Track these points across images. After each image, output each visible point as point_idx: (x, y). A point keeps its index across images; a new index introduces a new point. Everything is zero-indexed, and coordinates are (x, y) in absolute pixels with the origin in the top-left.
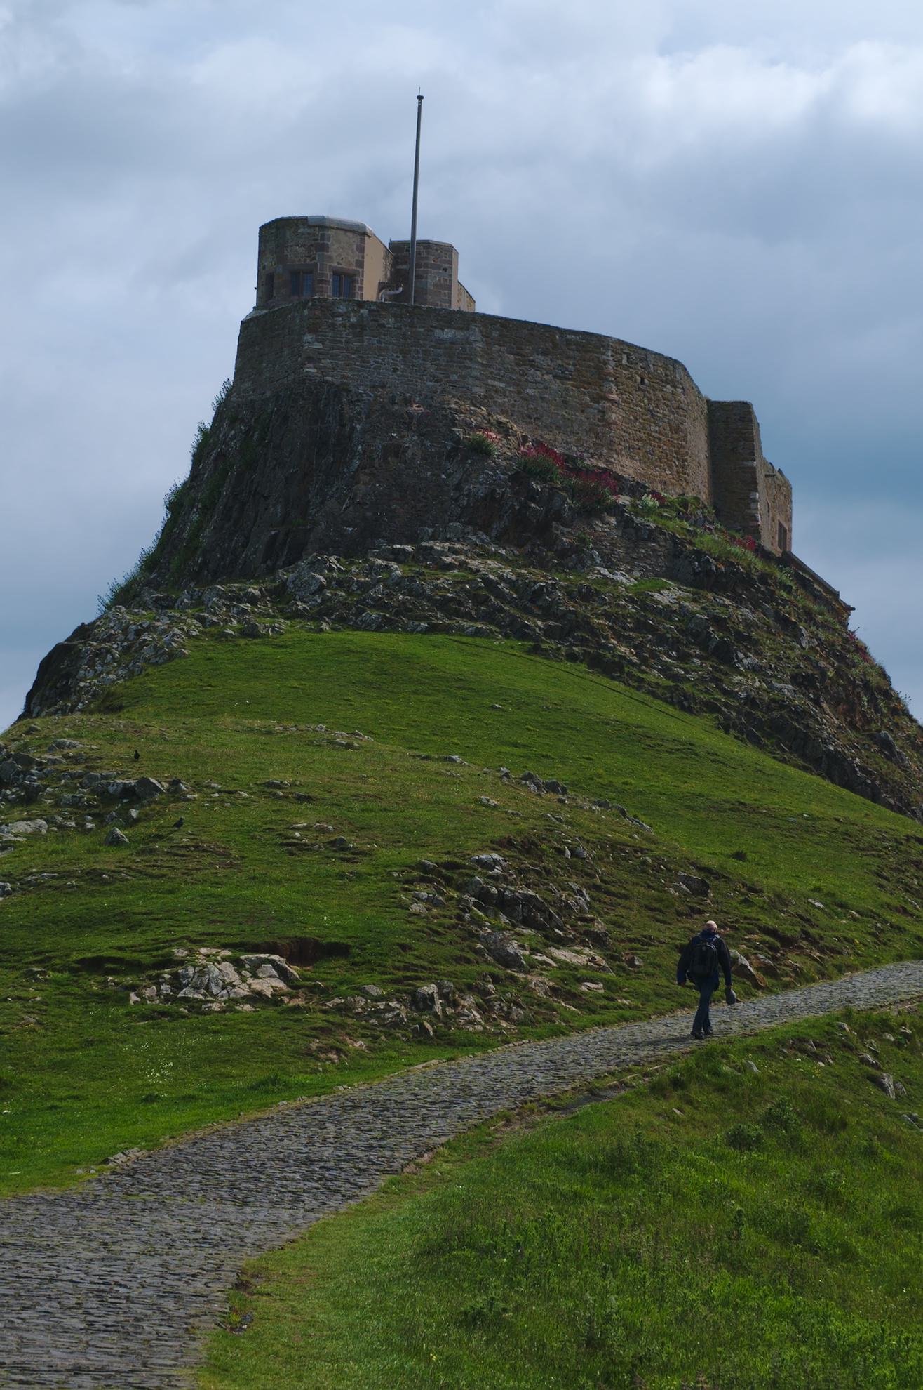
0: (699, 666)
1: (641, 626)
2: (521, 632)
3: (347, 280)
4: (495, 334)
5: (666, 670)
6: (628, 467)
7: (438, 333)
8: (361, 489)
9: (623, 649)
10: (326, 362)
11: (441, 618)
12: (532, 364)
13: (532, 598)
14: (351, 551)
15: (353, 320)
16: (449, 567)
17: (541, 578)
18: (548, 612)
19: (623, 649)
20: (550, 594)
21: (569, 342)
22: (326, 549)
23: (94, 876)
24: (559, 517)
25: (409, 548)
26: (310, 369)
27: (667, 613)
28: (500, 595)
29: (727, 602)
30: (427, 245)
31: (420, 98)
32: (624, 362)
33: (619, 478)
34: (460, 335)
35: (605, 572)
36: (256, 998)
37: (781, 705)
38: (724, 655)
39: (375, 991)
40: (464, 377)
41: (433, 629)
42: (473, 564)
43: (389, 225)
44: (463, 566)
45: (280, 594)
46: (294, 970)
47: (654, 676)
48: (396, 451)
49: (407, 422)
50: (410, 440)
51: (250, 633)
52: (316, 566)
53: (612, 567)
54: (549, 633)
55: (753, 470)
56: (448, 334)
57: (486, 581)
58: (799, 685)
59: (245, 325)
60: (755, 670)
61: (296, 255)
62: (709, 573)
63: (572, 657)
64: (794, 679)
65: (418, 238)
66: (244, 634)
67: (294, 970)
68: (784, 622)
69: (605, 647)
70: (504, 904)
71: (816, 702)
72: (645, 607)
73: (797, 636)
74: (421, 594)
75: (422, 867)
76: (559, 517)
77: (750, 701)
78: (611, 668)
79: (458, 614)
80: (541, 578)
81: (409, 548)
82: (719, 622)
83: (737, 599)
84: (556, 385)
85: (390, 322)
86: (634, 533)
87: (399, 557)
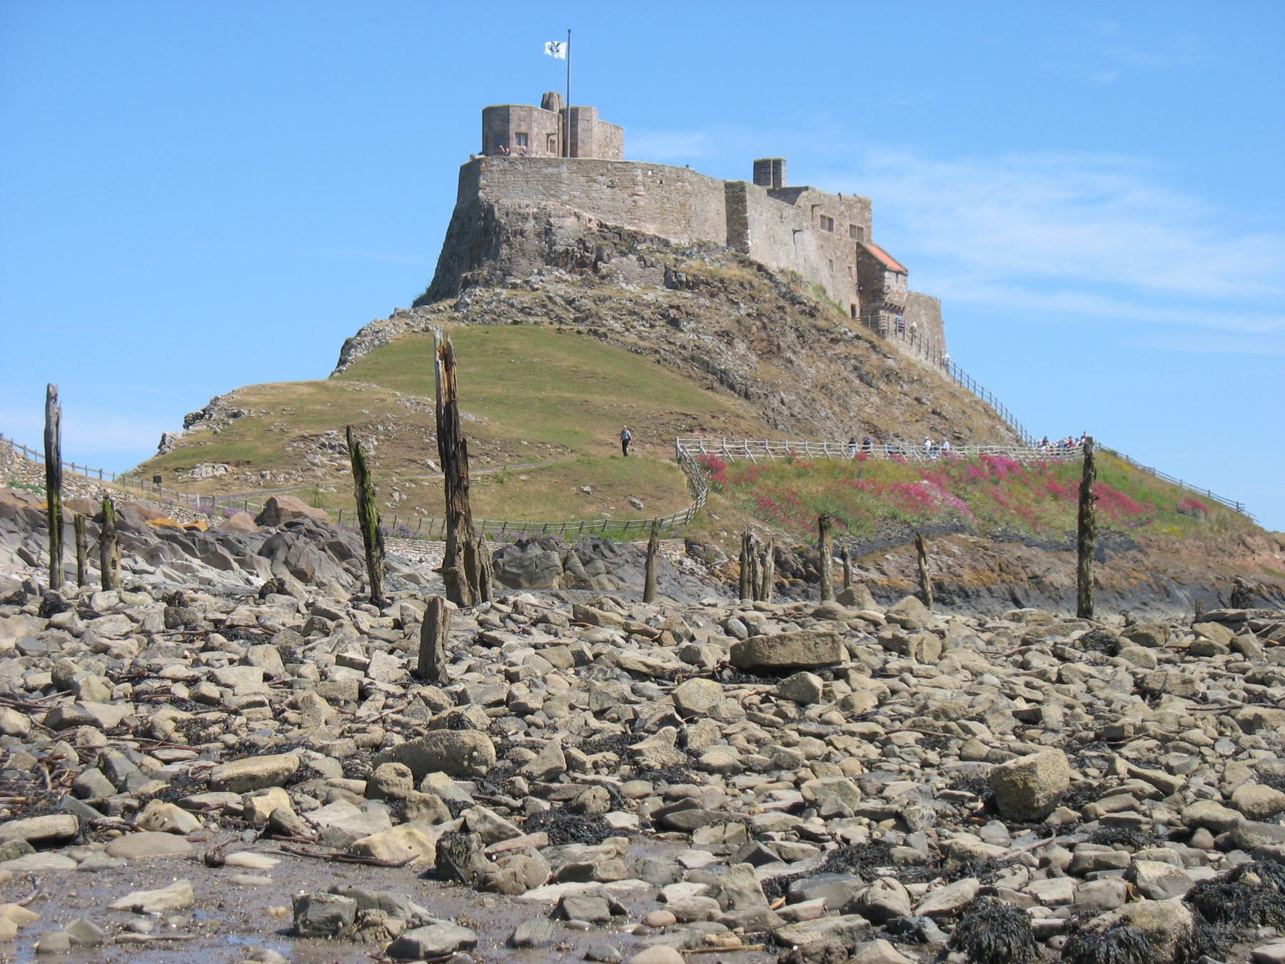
0: (661, 328)
3: (523, 137)
6: (650, 229)
7: (545, 171)
8: (505, 251)
10: (488, 190)
11: (520, 317)
18: (577, 309)
22: (487, 284)
24: (601, 259)
25: (519, 281)
26: (481, 194)
28: (555, 303)
29: (689, 295)
30: (575, 112)
35: (624, 285)
36: (214, 477)
41: (515, 323)
42: (549, 287)
46: (229, 469)
47: (632, 338)
48: (522, 233)
49: (525, 218)
50: (530, 226)
55: (746, 219)
56: (550, 170)
57: (550, 298)
61: (497, 127)
62: (681, 282)
71: (729, 343)
74: (512, 306)
76: (601, 259)
77: (684, 348)
79: (529, 314)
85: (521, 167)
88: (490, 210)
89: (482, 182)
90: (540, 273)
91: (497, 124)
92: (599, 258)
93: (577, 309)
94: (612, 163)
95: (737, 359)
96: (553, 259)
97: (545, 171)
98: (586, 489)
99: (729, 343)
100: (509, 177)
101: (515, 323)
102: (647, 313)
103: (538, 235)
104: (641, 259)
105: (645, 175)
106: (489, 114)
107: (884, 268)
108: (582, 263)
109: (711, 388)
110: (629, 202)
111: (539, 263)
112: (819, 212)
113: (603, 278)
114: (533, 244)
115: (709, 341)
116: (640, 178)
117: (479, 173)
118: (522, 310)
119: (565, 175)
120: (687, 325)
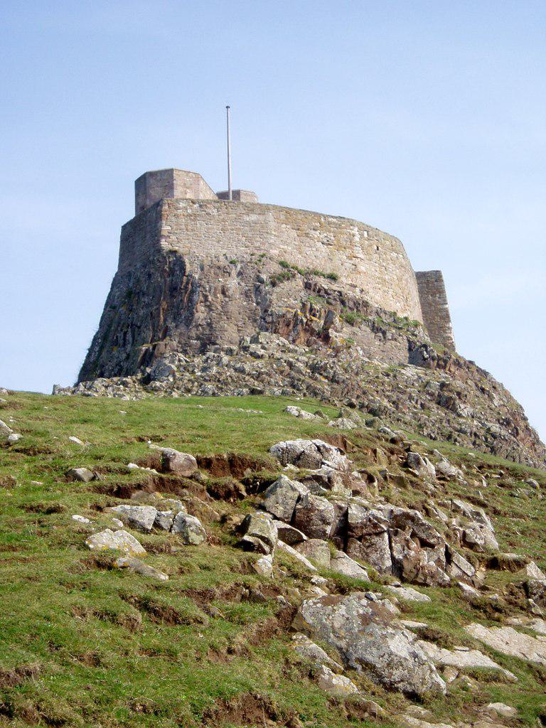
0: (437, 412)
4: (282, 217)
6: (376, 298)
7: (246, 218)
8: (201, 314)
9: (385, 402)
10: (173, 237)
12: (307, 235)
15: (189, 211)
18: (333, 380)
20: (332, 368)
21: (329, 223)
26: (164, 244)
28: (299, 372)
31: (227, 107)
32: (366, 235)
34: (262, 218)
40: (264, 244)
45: (146, 381)
50: (233, 283)
55: (446, 311)
56: (254, 217)
58: (502, 424)
59: (124, 227)
65: (232, 188)
68: (483, 390)
73: (491, 398)
82: (443, 385)
83: (453, 376)
84: (324, 248)
88: (180, 263)
89: (165, 228)
90: (255, 340)
91: (155, 192)
92: (329, 322)
93: (333, 380)
94: (325, 217)
96: (267, 321)
97: (246, 218)
100: (201, 225)
101: (253, 392)
102: (413, 391)
103: (246, 295)
104: (375, 329)
105: (362, 235)
106: (142, 184)
108: (309, 330)
110: (348, 264)
111: (251, 330)
113: (337, 351)
114: (238, 304)
115: (495, 428)
116: (357, 239)
117: (159, 217)
118: (258, 376)
119: (272, 224)
120: (465, 409)
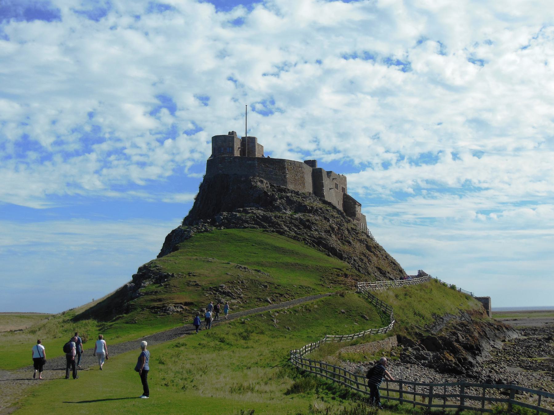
1: (291, 223)
2: (264, 227)
5: (295, 232)
6: (291, 187)
13: (266, 219)
14: (230, 210)
16: (250, 213)
17: (269, 214)
19: (286, 228)
23: (156, 292)
27: (296, 219)
33: (288, 190)
36: (177, 312)
37: (321, 238)
38: (309, 228)
39: (195, 310)
41: (245, 228)
43: (241, 134)
44: (252, 212)
47: (293, 234)
51: (206, 231)
52: (222, 215)
53: (286, 210)
54: (269, 226)
56: (250, 162)
57: (257, 216)
59: (208, 161)
60: (316, 230)
63: (273, 231)
64: (325, 232)
66: (205, 231)
67: (184, 307)
69: (282, 229)
70: (224, 293)
71: (330, 236)
72: (292, 219)
73: (329, 221)
75: (210, 288)
78: (282, 233)
80: (269, 214)
81: (241, 209)
82: (308, 221)
83: (314, 214)
86: (290, 202)
87: (239, 211)
95: (334, 241)
98: (343, 311)
99: (330, 236)
102: (297, 223)
107: (355, 202)
109: (329, 255)
112: (335, 181)
115: (323, 234)
